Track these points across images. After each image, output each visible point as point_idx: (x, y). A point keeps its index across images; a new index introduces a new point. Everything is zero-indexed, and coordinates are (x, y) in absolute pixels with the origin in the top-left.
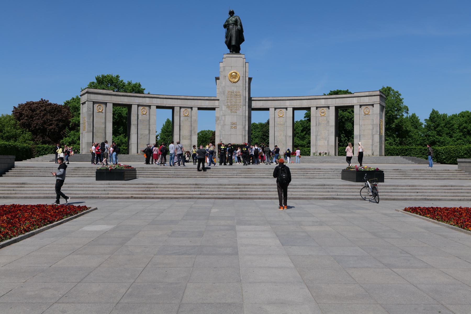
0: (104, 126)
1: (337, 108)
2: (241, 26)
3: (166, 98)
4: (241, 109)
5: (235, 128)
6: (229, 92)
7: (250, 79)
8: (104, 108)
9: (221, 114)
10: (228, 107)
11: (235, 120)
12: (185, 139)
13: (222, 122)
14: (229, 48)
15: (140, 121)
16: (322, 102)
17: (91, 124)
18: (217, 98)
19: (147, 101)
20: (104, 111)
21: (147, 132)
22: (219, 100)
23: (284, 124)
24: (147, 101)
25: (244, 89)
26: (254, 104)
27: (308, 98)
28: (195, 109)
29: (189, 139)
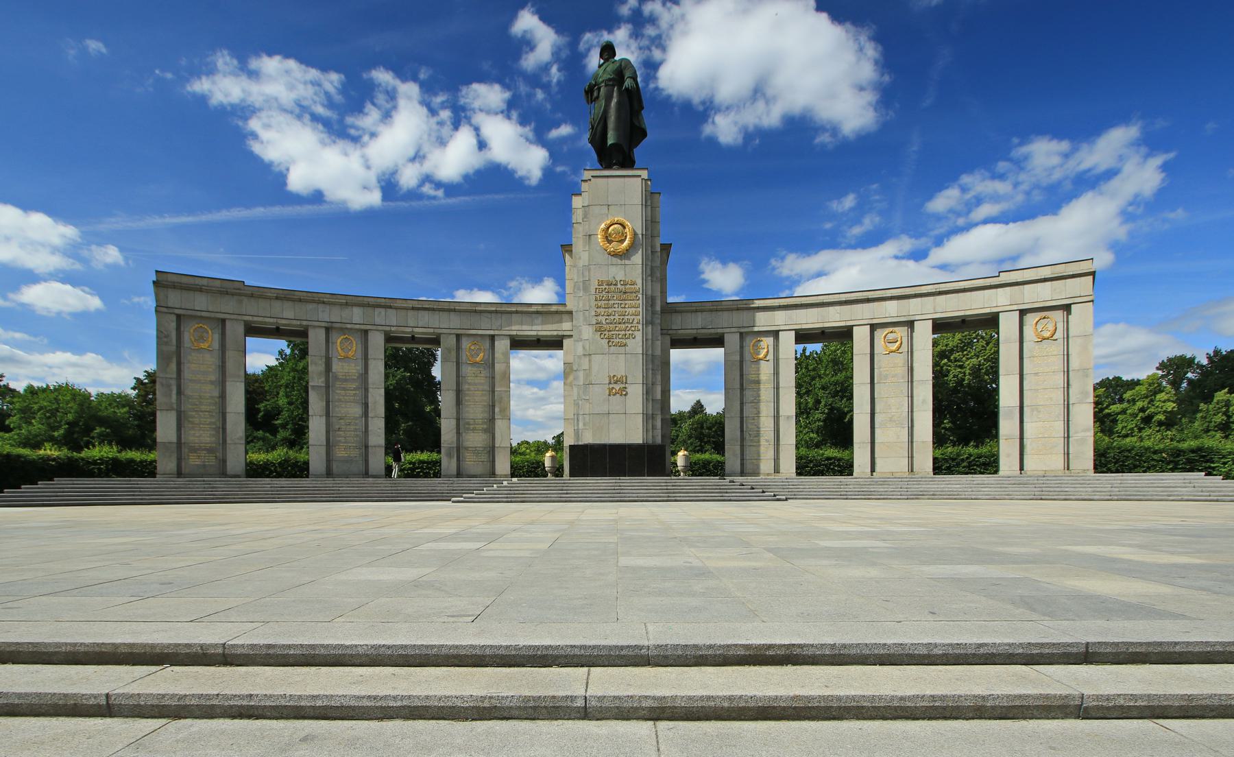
0: (216, 394)
1: (939, 326)
3: (413, 308)
4: (639, 335)
5: (623, 392)
6: (601, 283)
7: (666, 248)
8: (217, 337)
9: (580, 351)
10: (599, 329)
11: (620, 373)
12: (474, 429)
13: (581, 374)
15: (336, 378)
16: (891, 310)
17: (169, 386)
19: (357, 316)
20: (216, 345)
21: (356, 410)
24: (357, 316)
27: (843, 298)
29: (485, 431)
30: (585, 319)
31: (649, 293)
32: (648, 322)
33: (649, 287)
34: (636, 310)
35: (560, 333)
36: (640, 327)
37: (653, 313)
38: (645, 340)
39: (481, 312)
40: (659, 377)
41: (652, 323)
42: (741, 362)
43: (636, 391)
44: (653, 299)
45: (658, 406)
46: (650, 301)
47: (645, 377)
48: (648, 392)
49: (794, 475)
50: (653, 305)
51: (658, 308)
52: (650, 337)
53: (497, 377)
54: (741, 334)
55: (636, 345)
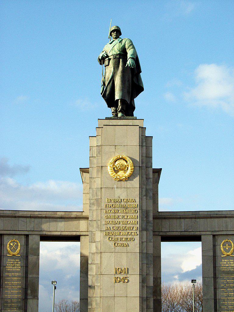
2: (136, 59)
4: (137, 238)
5: (125, 280)
9: (94, 250)
10: (108, 233)
11: (124, 265)
12: (11, 307)
14: (109, 106)
18: (84, 214)
22: (86, 218)
25: (144, 193)
26: (167, 227)
28: (33, 239)
29: (20, 308)
30: (98, 227)
31: (144, 208)
32: (143, 229)
33: (144, 204)
34: (134, 220)
35: (78, 234)
36: (138, 233)
37: (148, 222)
38: (141, 243)
39: (19, 217)
40: (151, 270)
41: (147, 230)
42: (215, 256)
43: (135, 280)
44: (147, 212)
45: (151, 291)
46: (144, 215)
47: (141, 270)
48: (143, 281)
50: (147, 217)
51: (151, 219)
52: (145, 240)
53: (30, 266)
54: (214, 236)
55: (135, 246)
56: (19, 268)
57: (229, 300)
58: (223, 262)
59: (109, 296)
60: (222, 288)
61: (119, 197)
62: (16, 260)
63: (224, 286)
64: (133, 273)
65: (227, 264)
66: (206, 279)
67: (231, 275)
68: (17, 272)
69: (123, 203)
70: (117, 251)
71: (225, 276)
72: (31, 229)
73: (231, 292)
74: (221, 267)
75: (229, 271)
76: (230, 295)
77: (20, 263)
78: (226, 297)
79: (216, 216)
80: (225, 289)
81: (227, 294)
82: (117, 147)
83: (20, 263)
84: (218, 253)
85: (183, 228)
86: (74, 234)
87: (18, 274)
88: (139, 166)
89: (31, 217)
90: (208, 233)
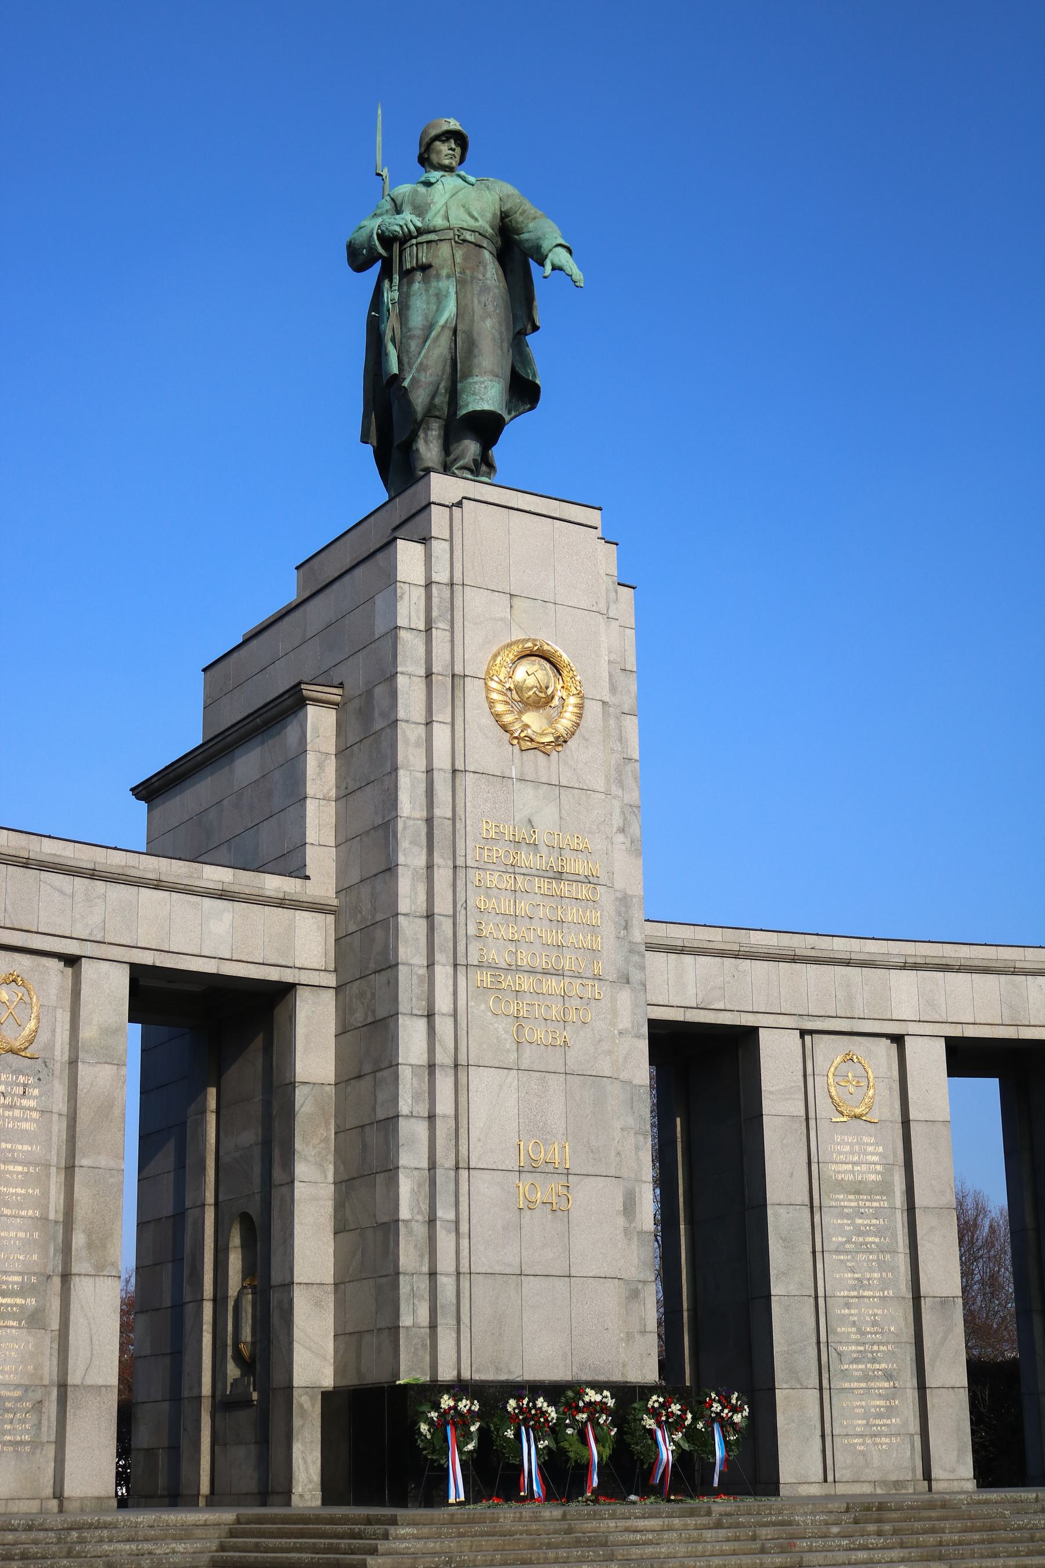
23: (883, 1188)
29: (34, 1320)
35: (288, 976)
49: (971, 1485)
56: (34, 1120)
57: (866, 1300)
58: (838, 1143)
59: (497, 1269)
60: (837, 1252)
61: (530, 821)
62: (22, 1079)
63: (844, 1244)
64: (591, 1171)
65: (852, 1153)
66: (782, 1211)
67: (867, 1200)
68: (23, 1136)
69: (544, 850)
70: (525, 1064)
71: (849, 1202)
72: (91, 934)
73: (871, 1270)
74: (833, 1167)
75: (860, 1182)
76: (869, 1280)
77: (36, 1092)
78: (854, 1288)
79: (813, 953)
80: (849, 1257)
81: (856, 1276)
82: (516, 601)
83: (36, 1092)
84: (823, 1108)
85: (691, 991)
86: (273, 975)
87: (26, 1148)
88: (604, 703)
89: (93, 875)
90: (784, 1021)
